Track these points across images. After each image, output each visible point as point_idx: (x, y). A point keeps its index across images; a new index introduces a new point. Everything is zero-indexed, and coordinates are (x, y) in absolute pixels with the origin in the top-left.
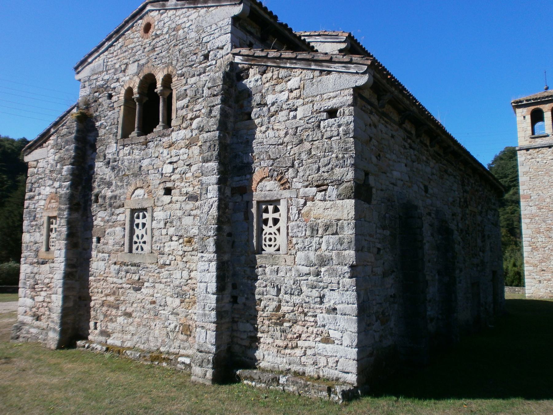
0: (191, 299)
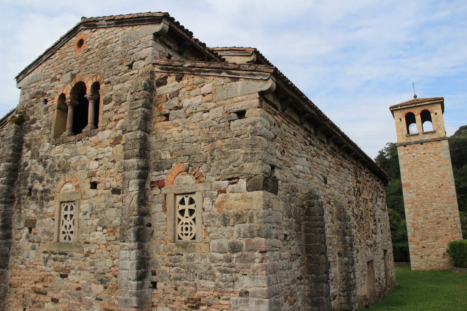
0: (114, 285)
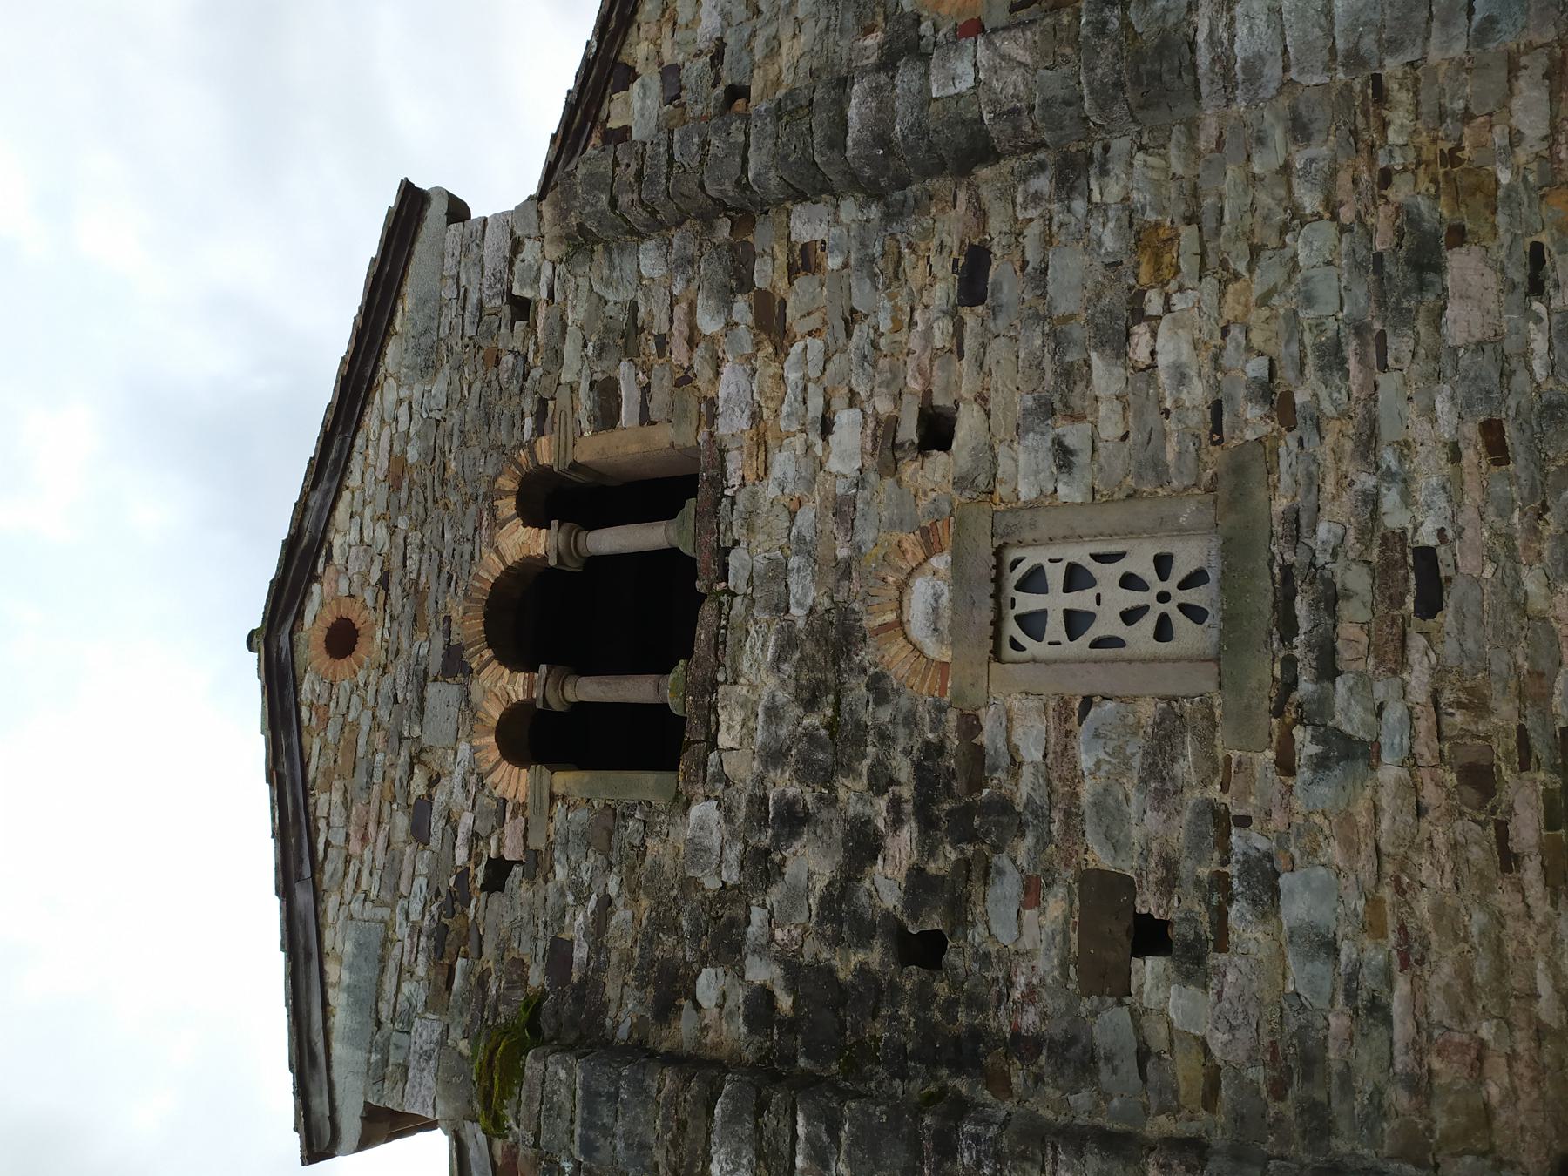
0: (1434, 181)
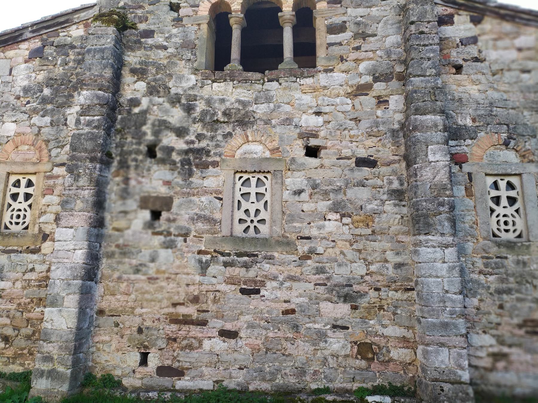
0: (374, 303)
